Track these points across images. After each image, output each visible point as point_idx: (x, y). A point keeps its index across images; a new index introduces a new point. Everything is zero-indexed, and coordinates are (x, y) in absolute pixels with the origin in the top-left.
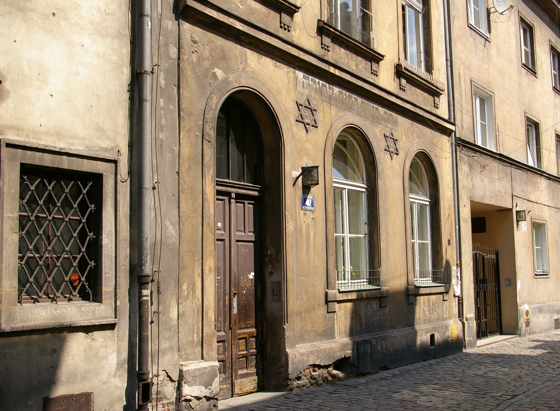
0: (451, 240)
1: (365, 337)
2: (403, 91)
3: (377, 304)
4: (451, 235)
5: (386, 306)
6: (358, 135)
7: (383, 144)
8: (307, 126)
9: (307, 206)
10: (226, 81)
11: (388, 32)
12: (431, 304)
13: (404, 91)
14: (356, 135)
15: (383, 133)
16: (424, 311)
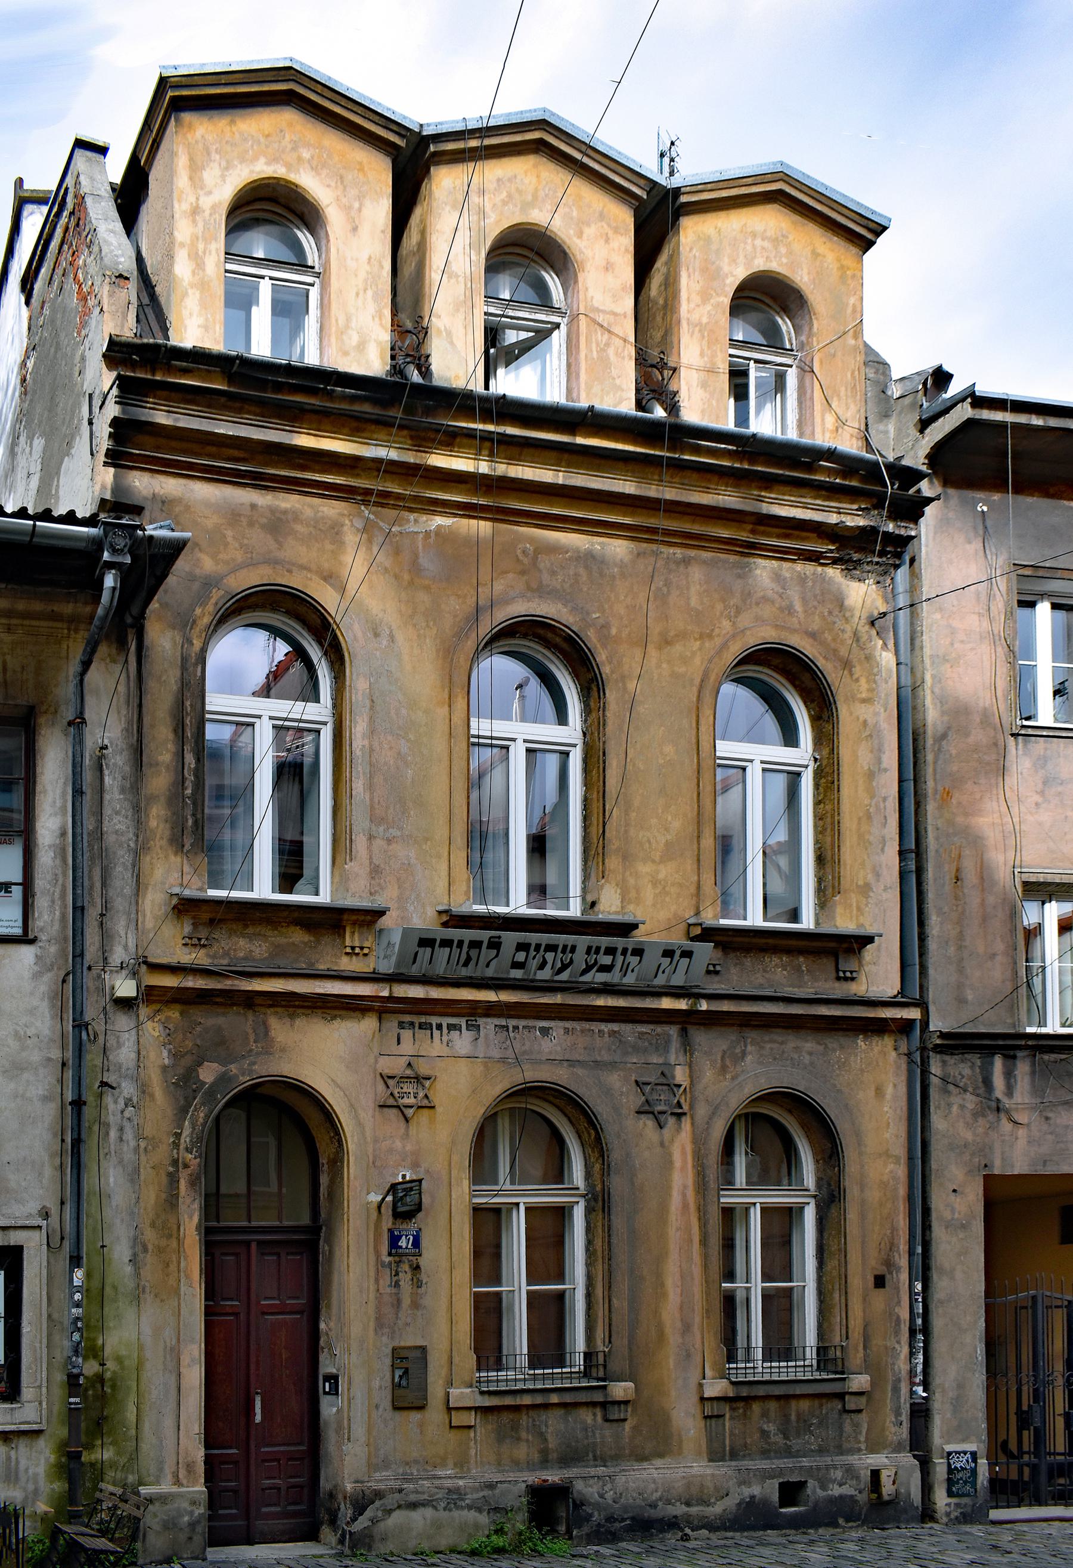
0: (888, 1277)
1: (553, 1476)
2: (713, 976)
3: (595, 1415)
4: (889, 1263)
5: (625, 1420)
6: (554, 1097)
7: (633, 1100)
8: (409, 1112)
9: (401, 1247)
10: (223, 1079)
11: (661, 862)
12: (793, 1417)
13: (717, 973)
14: (551, 1099)
15: (633, 1078)
16: (764, 1434)
